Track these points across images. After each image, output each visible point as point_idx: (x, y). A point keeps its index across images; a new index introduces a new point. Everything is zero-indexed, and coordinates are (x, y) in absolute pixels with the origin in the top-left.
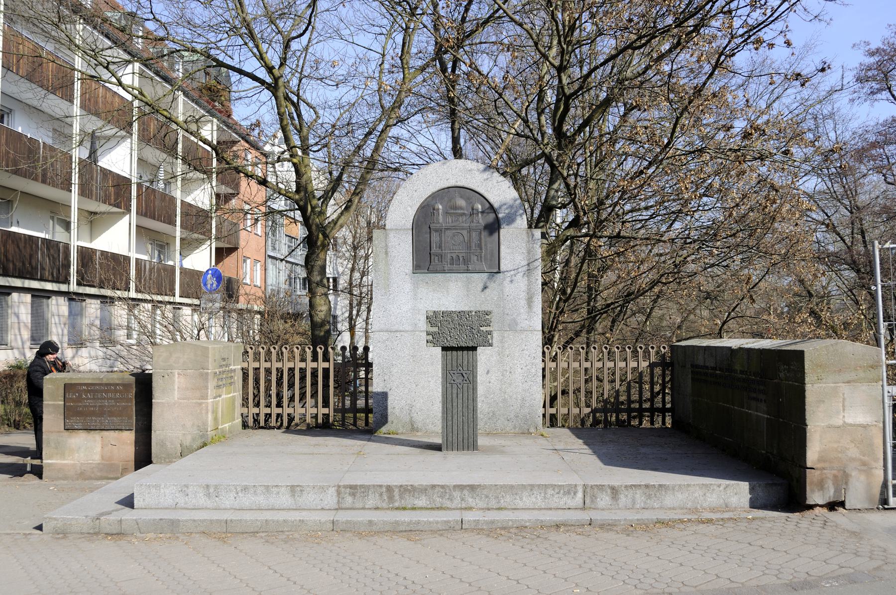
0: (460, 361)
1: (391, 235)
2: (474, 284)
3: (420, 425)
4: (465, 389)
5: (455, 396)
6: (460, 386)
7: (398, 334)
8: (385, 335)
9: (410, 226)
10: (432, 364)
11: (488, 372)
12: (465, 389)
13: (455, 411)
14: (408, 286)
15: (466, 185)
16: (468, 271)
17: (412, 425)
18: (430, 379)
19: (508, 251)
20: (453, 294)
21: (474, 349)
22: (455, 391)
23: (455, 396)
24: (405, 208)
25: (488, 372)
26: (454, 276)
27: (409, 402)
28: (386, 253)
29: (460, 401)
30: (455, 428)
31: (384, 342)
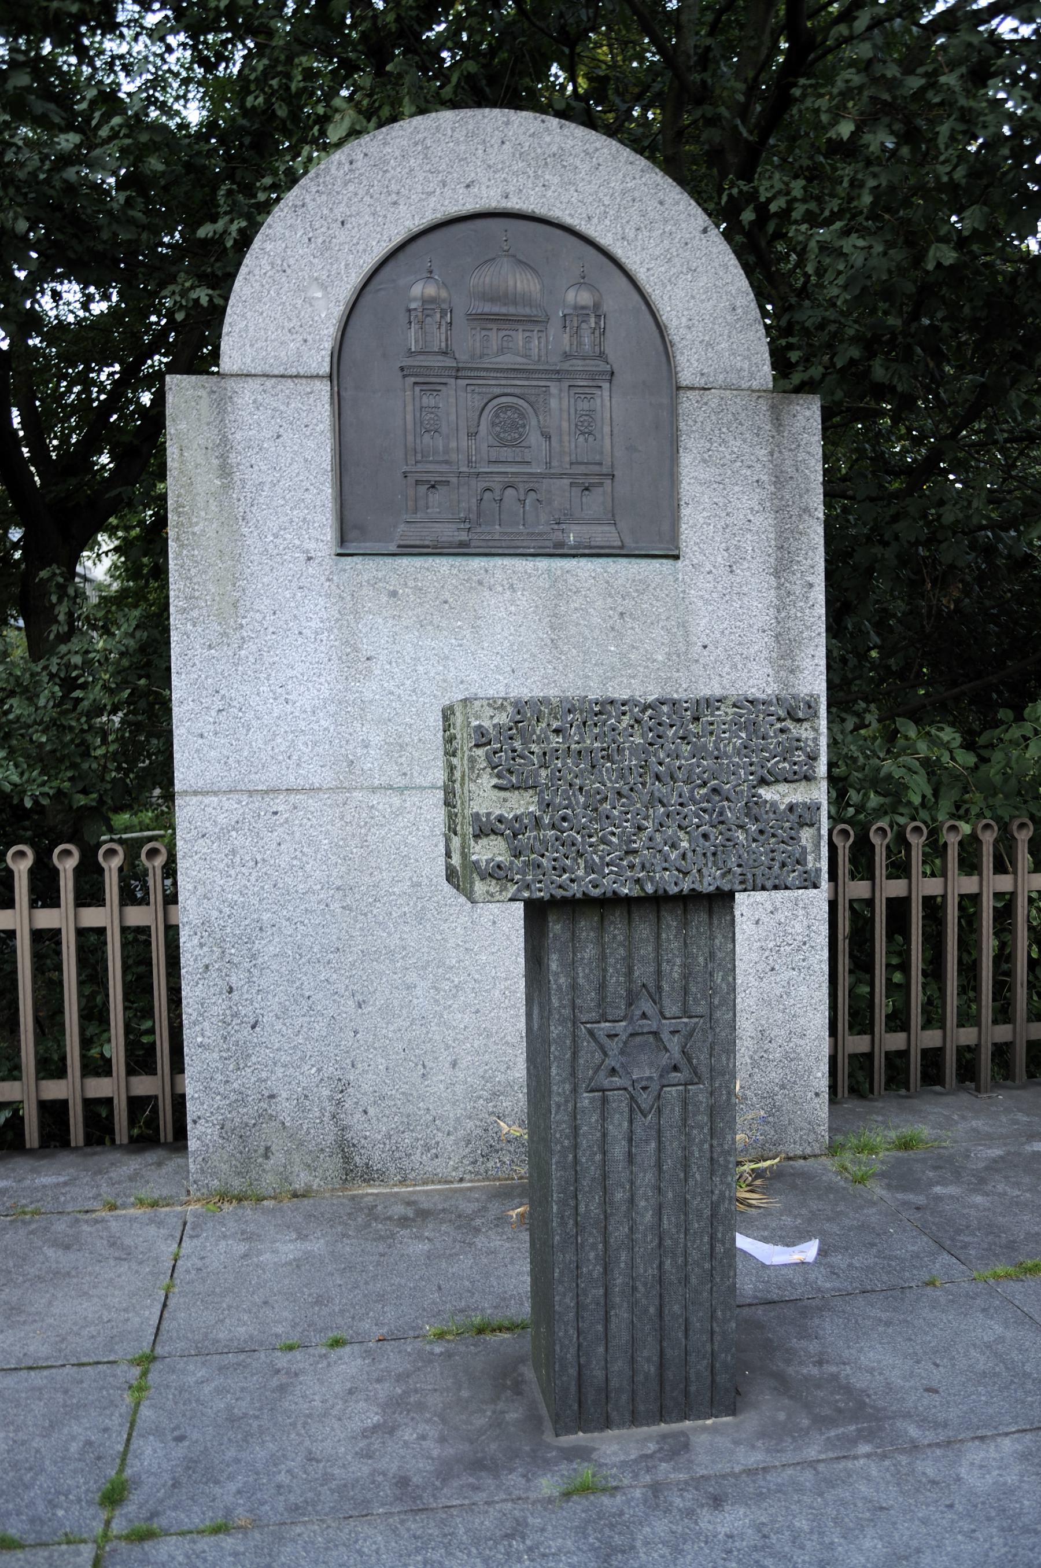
0: (643, 973)
1: (246, 394)
2: (577, 602)
3: (377, 1157)
4: (673, 1114)
5: (618, 1151)
6: (645, 1099)
7: (280, 803)
9: (320, 361)
10: (420, 918)
13: (619, 1232)
14: (316, 610)
15: (541, 211)
16: (560, 551)
17: (347, 1159)
18: (412, 977)
20: (513, 631)
21: (721, 901)
22: (617, 1127)
23: (618, 1151)
24: (300, 289)
26: (502, 569)
27: (329, 1070)
28: (225, 471)
29: (646, 1178)
30: (621, 1315)
31: (224, 832)
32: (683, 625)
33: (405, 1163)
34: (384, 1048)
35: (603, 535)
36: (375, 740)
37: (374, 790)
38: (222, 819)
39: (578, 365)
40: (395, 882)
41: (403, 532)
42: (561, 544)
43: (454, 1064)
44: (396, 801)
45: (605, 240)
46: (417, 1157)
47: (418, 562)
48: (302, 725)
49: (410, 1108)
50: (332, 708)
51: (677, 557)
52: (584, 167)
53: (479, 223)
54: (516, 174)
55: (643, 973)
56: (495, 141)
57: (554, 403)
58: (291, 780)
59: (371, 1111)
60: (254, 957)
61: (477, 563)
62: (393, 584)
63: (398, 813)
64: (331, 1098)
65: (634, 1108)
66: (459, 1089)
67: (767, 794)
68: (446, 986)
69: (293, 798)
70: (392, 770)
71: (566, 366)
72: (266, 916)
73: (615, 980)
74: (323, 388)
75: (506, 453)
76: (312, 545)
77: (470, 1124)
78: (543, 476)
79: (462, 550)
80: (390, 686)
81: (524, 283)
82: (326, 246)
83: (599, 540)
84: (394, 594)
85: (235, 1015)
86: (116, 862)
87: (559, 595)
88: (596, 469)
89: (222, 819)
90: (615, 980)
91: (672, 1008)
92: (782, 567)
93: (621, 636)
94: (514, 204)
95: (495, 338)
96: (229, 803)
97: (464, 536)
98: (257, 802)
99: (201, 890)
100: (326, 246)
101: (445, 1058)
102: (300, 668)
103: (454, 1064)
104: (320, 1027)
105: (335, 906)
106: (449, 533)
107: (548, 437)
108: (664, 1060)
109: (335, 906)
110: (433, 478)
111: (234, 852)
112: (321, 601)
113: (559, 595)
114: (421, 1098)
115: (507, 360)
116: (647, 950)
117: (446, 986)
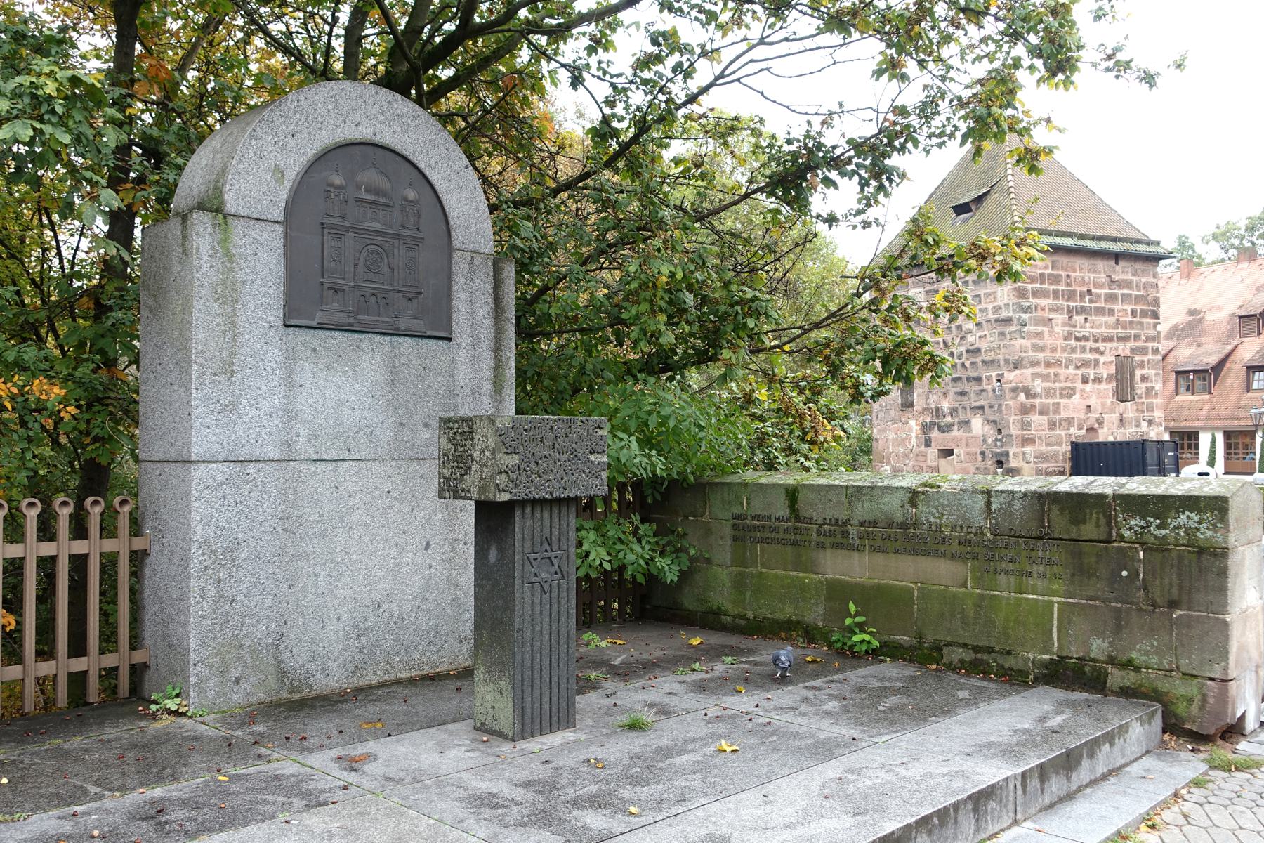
0: (546, 532)
4: (555, 592)
6: (546, 587)
7: (251, 468)
8: (219, 472)
10: (323, 535)
11: (427, 546)
12: (555, 592)
14: (273, 357)
18: (318, 569)
19: (464, 296)
22: (537, 600)
25: (427, 546)
29: (546, 620)
31: (220, 484)
32: (452, 375)
33: (312, 681)
34: (302, 613)
35: (417, 325)
36: (303, 432)
37: (301, 461)
38: (218, 477)
39: (407, 232)
40: (311, 514)
41: (320, 317)
42: (398, 329)
43: (338, 620)
44: (313, 468)
45: (422, 166)
46: (317, 677)
47: (327, 333)
48: (265, 422)
49: (315, 647)
50: (281, 413)
51: (450, 340)
52: (413, 124)
53: (362, 147)
54: (380, 122)
55: (546, 532)
56: (370, 102)
57: (396, 251)
58: (258, 454)
59: (294, 650)
60: (233, 560)
61: (355, 336)
62: (314, 344)
63: (314, 474)
64: (273, 644)
65: (542, 589)
66: (341, 633)
67: (592, 458)
68: (335, 574)
69: (258, 465)
70: (311, 449)
71: (401, 232)
72: (241, 536)
73: (537, 535)
74: (279, 228)
75: (371, 276)
76: (272, 319)
77: (346, 654)
78: (390, 291)
79: (350, 329)
80: (311, 402)
81: (382, 183)
82: (284, 147)
83: (417, 327)
84: (314, 350)
85: (222, 596)
86: (97, 510)
87: (395, 356)
88: (415, 290)
89: (218, 477)
90: (537, 535)
91: (555, 547)
92: (497, 349)
93: (423, 379)
94: (379, 139)
95: (370, 213)
96: (223, 467)
97: (351, 321)
98: (238, 467)
99: (205, 520)
100: (284, 147)
101: (334, 616)
102: (264, 389)
103: (338, 620)
104: (268, 601)
105: (279, 529)
106: (342, 318)
107: (392, 270)
108: (553, 569)
109: (279, 529)
110: (337, 287)
111: (224, 497)
112: (276, 351)
113: (395, 356)
114: (321, 641)
115: (374, 225)
116: (547, 522)
117: (335, 574)
